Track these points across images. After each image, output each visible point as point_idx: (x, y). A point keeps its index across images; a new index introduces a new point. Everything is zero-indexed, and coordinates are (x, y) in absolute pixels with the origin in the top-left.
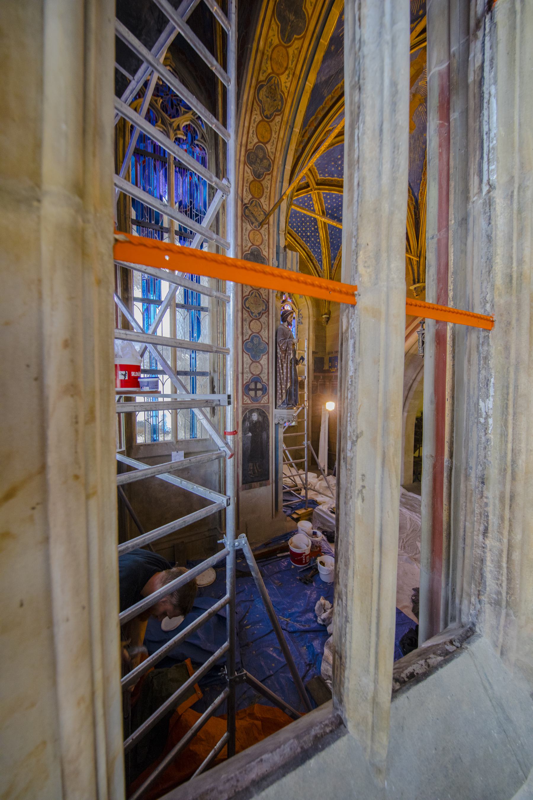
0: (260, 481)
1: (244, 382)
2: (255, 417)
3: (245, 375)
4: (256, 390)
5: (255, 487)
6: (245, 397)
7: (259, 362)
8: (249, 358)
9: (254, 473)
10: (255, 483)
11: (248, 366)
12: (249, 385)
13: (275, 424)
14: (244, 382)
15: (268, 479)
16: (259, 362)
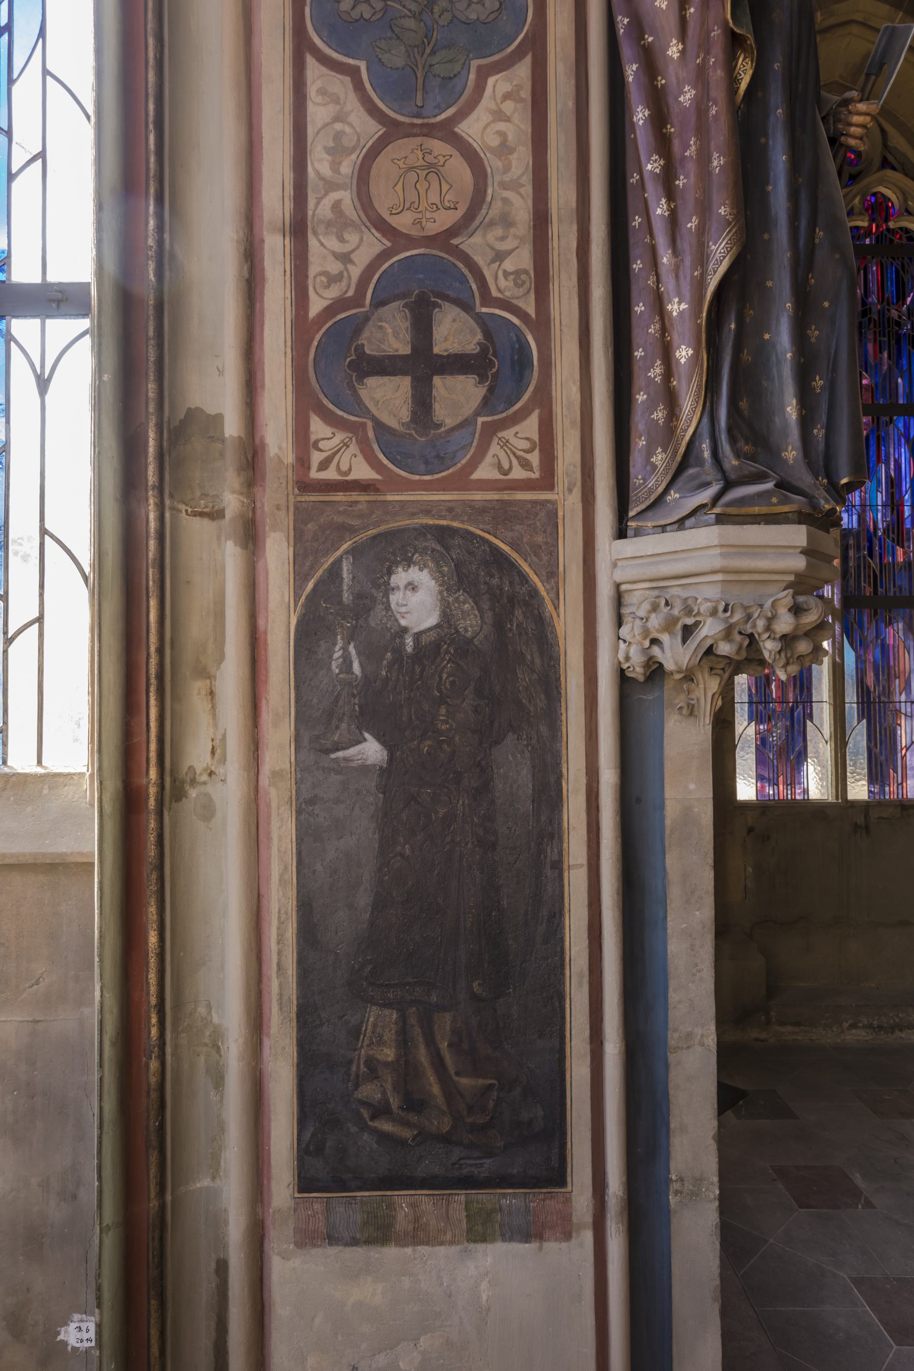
0: (468, 1182)
1: (316, 306)
2: (417, 600)
3: (322, 250)
4: (423, 365)
5: (418, 1235)
6: (318, 427)
7: (447, 132)
8: (352, 102)
9: (415, 1103)
10: (425, 1199)
11: (348, 167)
12: (358, 326)
13: (623, 678)
14: (316, 306)
15: (557, 1177)
16: (447, 132)
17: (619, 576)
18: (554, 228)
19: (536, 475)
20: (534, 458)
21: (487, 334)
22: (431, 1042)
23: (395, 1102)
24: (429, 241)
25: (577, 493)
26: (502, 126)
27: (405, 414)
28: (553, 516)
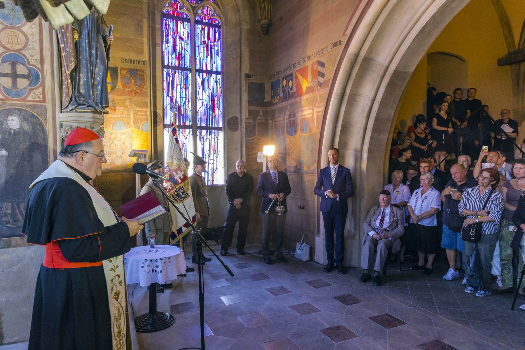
5: (17, 245)
9: (16, 221)
10: (18, 239)
16: (19, 29)
17: (61, 120)
18: (45, 52)
19: (41, 100)
20: (41, 96)
21: (29, 71)
22: (19, 209)
23: (11, 221)
24: (15, 51)
25: (51, 104)
26: (32, 30)
27: (10, 85)
28: (45, 108)
